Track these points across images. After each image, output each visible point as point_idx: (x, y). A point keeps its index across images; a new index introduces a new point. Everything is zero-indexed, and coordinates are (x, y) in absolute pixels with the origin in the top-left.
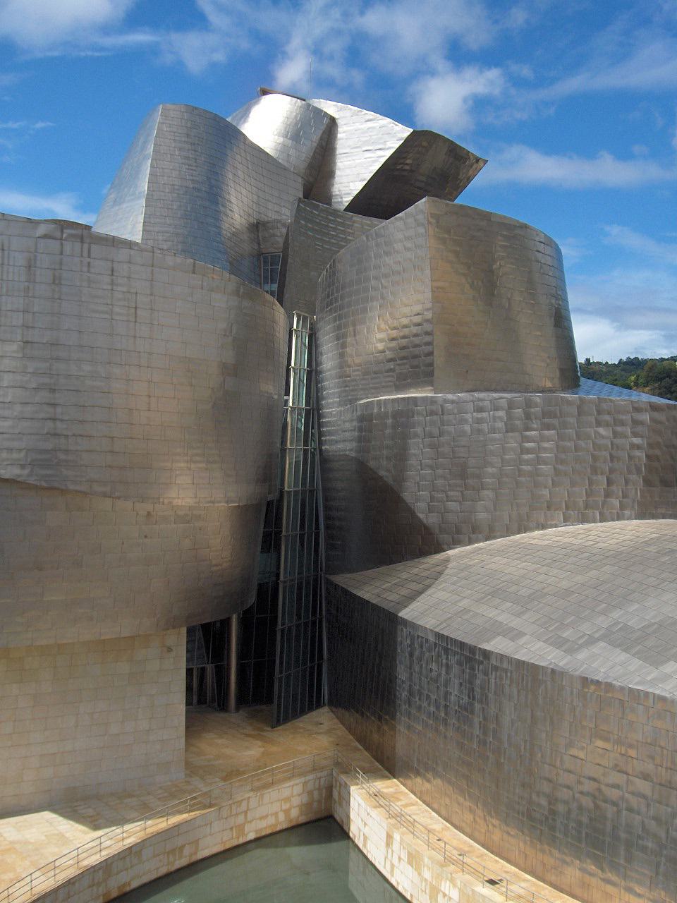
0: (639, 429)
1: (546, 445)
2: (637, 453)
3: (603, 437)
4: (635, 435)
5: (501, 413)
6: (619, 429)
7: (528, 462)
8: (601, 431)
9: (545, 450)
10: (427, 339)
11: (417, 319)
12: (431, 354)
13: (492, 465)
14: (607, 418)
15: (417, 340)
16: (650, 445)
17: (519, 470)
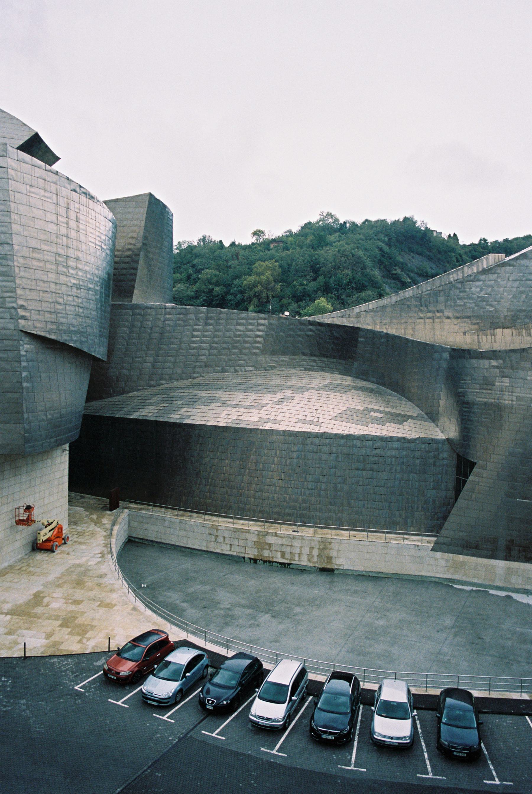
0: (261, 327)
1: (207, 333)
2: (258, 339)
3: (240, 331)
4: (259, 330)
5: (181, 316)
6: (250, 327)
7: (194, 342)
8: (239, 328)
9: (205, 336)
10: (133, 271)
11: (128, 260)
12: (134, 280)
13: (173, 343)
14: (244, 321)
15: (124, 272)
16: (267, 335)
17: (190, 346)
